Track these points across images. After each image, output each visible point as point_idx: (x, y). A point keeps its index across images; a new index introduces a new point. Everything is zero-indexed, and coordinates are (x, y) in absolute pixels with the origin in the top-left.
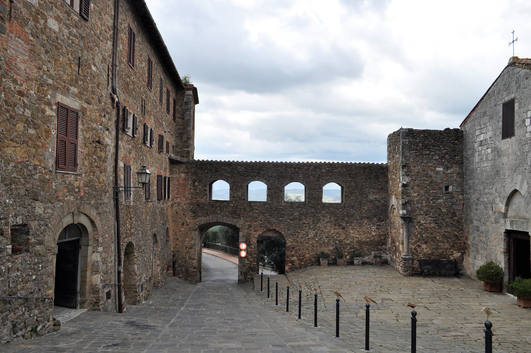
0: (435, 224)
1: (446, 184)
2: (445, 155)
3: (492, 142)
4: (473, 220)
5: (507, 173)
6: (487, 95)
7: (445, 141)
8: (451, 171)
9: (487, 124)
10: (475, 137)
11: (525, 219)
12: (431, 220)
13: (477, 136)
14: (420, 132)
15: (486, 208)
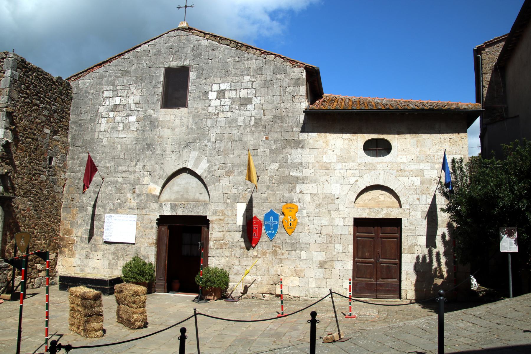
0: (35, 211)
1: (51, 154)
2: (54, 113)
3: (138, 109)
4: (87, 206)
5: (169, 149)
6: (132, 52)
7: (56, 93)
9: (130, 86)
10: (102, 99)
11: (197, 201)
12: (31, 204)
13: (106, 97)
14: (34, 69)
15: (119, 190)
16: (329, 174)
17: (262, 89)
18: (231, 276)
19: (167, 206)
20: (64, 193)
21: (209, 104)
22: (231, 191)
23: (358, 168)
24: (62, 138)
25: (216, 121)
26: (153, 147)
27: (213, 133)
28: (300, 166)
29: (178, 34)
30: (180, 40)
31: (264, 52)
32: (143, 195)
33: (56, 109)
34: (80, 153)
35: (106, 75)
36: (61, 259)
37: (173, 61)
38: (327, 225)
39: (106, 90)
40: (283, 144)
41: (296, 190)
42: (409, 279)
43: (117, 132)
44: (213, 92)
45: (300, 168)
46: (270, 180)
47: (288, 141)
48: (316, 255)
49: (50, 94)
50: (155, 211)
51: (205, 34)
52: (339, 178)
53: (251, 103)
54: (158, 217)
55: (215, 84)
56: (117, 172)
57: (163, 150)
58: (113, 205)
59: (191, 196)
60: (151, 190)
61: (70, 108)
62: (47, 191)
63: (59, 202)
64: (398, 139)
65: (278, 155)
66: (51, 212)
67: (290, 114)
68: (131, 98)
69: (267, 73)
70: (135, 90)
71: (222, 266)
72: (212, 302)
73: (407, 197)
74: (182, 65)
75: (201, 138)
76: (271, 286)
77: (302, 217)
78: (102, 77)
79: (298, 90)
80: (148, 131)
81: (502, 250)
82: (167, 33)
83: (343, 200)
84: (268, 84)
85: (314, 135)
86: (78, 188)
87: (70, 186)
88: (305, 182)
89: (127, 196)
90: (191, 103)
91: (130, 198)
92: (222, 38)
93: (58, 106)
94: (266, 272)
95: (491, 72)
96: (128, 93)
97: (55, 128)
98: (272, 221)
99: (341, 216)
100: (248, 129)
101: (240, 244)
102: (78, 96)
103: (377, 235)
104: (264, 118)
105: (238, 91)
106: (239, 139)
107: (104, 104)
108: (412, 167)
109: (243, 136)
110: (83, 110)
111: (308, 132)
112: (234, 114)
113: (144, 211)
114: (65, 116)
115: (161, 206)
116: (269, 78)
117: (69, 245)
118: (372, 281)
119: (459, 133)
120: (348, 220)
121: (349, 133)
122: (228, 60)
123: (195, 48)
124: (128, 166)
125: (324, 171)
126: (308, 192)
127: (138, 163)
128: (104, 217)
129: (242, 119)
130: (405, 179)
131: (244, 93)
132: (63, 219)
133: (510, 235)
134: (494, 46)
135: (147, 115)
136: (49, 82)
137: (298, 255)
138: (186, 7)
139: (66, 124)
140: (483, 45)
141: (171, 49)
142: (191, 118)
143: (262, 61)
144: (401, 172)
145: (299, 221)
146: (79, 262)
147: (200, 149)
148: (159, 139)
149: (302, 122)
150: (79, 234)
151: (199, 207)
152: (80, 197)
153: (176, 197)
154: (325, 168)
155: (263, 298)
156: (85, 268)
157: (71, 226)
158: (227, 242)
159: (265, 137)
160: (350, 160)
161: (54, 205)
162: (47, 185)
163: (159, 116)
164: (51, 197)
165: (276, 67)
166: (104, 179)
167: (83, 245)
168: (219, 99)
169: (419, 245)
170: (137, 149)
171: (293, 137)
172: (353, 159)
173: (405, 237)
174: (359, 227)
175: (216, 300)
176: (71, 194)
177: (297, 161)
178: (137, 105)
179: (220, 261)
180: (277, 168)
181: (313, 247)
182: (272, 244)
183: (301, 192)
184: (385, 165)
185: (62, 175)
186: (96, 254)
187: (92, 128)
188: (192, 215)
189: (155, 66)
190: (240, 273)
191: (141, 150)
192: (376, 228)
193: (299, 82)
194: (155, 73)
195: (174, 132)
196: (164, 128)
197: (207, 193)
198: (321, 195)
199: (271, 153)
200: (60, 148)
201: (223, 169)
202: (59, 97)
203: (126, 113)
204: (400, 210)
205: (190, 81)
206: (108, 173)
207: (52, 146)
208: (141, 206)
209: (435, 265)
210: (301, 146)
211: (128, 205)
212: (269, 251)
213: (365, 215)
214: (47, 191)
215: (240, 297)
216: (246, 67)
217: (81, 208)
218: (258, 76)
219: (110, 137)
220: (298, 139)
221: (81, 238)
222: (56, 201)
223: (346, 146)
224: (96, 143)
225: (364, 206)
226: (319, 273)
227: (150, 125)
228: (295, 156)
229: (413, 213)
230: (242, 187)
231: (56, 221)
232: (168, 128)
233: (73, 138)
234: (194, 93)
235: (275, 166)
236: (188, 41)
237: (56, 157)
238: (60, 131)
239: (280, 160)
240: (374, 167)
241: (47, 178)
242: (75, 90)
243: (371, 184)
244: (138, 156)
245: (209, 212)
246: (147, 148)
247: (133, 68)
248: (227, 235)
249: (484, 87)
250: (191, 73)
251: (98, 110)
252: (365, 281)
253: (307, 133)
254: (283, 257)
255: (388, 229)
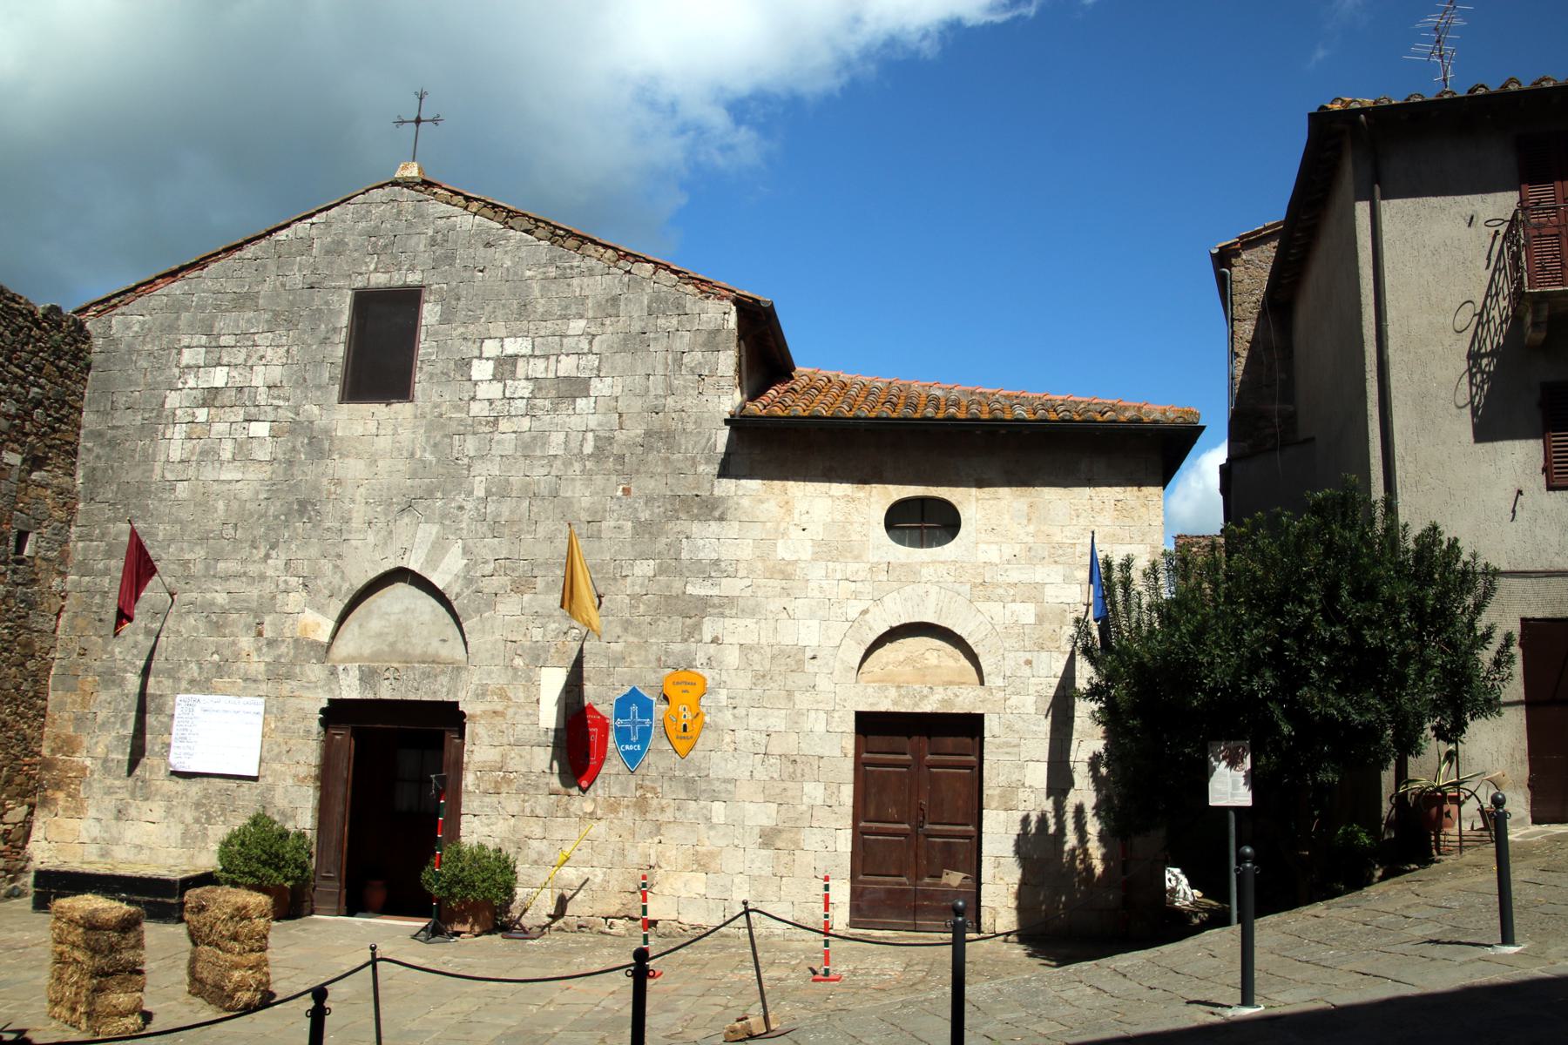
1: (23, 522)
2: (36, 407)
3: (276, 402)
4: (126, 671)
5: (359, 514)
6: (263, 242)
7: (41, 350)
8: (43, 477)
9: (256, 337)
10: (176, 371)
11: (433, 662)
13: (188, 367)
15: (217, 627)
16: (790, 591)
17: (618, 356)
18: (522, 869)
19: (351, 673)
20: (58, 632)
21: (472, 394)
22: (525, 635)
23: (869, 575)
24: (56, 477)
25: (491, 441)
26: (314, 510)
27: (480, 475)
28: (713, 569)
29: (395, 195)
30: (399, 213)
31: (627, 254)
32: (283, 641)
33: (40, 397)
34: (109, 520)
35: (188, 303)
36: (45, 823)
37: (376, 270)
38: (783, 730)
39: (188, 347)
40: (669, 507)
41: (701, 634)
42: (1001, 879)
43: (217, 465)
44: (484, 361)
45: (713, 574)
46: (632, 606)
47: (682, 501)
48: (752, 813)
49: (23, 354)
50: (316, 687)
51: (468, 199)
52: (818, 603)
53: (586, 394)
54: (325, 704)
55: (490, 338)
56: (214, 576)
57: (342, 517)
58: (200, 668)
59: (418, 646)
60: (305, 629)
61: (82, 394)
62: (6, 627)
63: (43, 659)
64: (977, 500)
65: (654, 537)
66: (17, 688)
67: (690, 427)
68: (259, 369)
69: (633, 314)
70: (269, 349)
71: (497, 840)
72: (467, 939)
73: (1000, 658)
74: (400, 283)
75: (449, 487)
76: (629, 896)
77: (717, 708)
78: (179, 309)
79: (713, 360)
80: (302, 463)
81: (1214, 801)
82: (363, 193)
83: (827, 664)
84: (635, 343)
85: (754, 485)
86: (100, 620)
87: (76, 615)
88: (727, 612)
89: (240, 645)
90: (424, 389)
91: (247, 649)
92: (512, 211)
93: (47, 387)
94: (616, 858)
95: (1256, 316)
96: (249, 356)
97: (37, 449)
98: (634, 717)
99: (821, 706)
100: (577, 466)
101: (547, 780)
102: (107, 360)
103: (918, 758)
104: (620, 436)
105: (553, 359)
106: (550, 492)
107: (180, 386)
108: (1015, 576)
109: (563, 483)
110: (121, 401)
111: (738, 477)
112: (538, 423)
113: (286, 687)
114: (67, 417)
115: (332, 674)
116: (636, 327)
117: (68, 781)
118: (905, 884)
119: (1140, 485)
120: (840, 717)
121: (848, 482)
122: (528, 273)
123: (439, 237)
124: (244, 561)
125: (777, 583)
126: (734, 640)
127: (274, 554)
128: (171, 703)
129: (562, 436)
130: (995, 608)
131: (567, 366)
132: (55, 706)
133: (1233, 762)
134: (1264, 247)
135: (301, 418)
136: (20, 319)
137: (704, 811)
138: (418, 121)
139: (72, 440)
140: (1236, 243)
141: (373, 239)
142: (422, 431)
143: (621, 280)
144: (983, 588)
145: (707, 719)
146: (96, 830)
147: (444, 516)
148: (333, 488)
149: (724, 450)
150: (100, 750)
151: (438, 679)
152: (106, 644)
153: (375, 648)
154: (781, 576)
155: (608, 930)
156: (114, 847)
157: (77, 728)
158: (512, 776)
159: (621, 487)
160: (848, 555)
161: (26, 669)
162: (8, 611)
163: (335, 422)
164: (19, 645)
165: (657, 298)
166: (175, 597)
167: (108, 782)
168: (500, 381)
169: (1030, 787)
170: (271, 512)
171: (698, 488)
172: (856, 553)
173: (991, 766)
174: (870, 737)
175: (476, 936)
176: (79, 637)
177: (707, 555)
178: (275, 392)
179: (494, 827)
180: (652, 574)
181: (744, 790)
182: (633, 781)
183: (715, 640)
184: (942, 569)
185: (56, 582)
186: (145, 806)
187: (144, 450)
188: (418, 699)
189: (326, 284)
190: (546, 859)
191: (283, 517)
192: (915, 739)
193: (719, 339)
194: (327, 303)
195: (375, 469)
196: (347, 456)
197: (460, 638)
198: (769, 650)
199: (636, 533)
200: (50, 507)
201: (506, 575)
202: (52, 363)
203: (242, 412)
204: (979, 691)
205: (423, 329)
206: (188, 578)
207: (27, 500)
208: (278, 673)
209: (1071, 840)
210: (717, 514)
211: (242, 671)
212: (626, 801)
213: (885, 705)
214: (6, 627)
215: (544, 927)
216: (577, 294)
217: (107, 677)
218: (608, 322)
219: (197, 479)
220: (712, 494)
221: (105, 761)
222: (33, 656)
223: (839, 517)
224: (156, 495)
225: (884, 681)
226: (761, 860)
227: (308, 448)
228: (701, 543)
229: (1014, 700)
230: (557, 625)
231: (31, 713)
232: (358, 456)
233: (91, 477)
234: (432, 364)
235: (645, 568)
236: (421, 216)
237: (39, 531)
238: (51, 459)
239: (659, 553)
240: (911, 575)
241: (8, 591)
242: (98, 343)
243: (905, 620)
244: (272, 533)
245: (464, 693)
246: (298, 511)
247: (266, 288)
248: (513, 755)
249: (1237, 355)
250: (425, 306)
251: (164, 402)
252: (885, 883)
253: (733, 481)
254: (662, 818)
255: (949, 742)
